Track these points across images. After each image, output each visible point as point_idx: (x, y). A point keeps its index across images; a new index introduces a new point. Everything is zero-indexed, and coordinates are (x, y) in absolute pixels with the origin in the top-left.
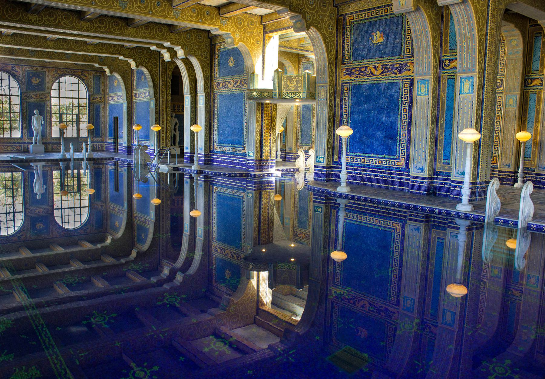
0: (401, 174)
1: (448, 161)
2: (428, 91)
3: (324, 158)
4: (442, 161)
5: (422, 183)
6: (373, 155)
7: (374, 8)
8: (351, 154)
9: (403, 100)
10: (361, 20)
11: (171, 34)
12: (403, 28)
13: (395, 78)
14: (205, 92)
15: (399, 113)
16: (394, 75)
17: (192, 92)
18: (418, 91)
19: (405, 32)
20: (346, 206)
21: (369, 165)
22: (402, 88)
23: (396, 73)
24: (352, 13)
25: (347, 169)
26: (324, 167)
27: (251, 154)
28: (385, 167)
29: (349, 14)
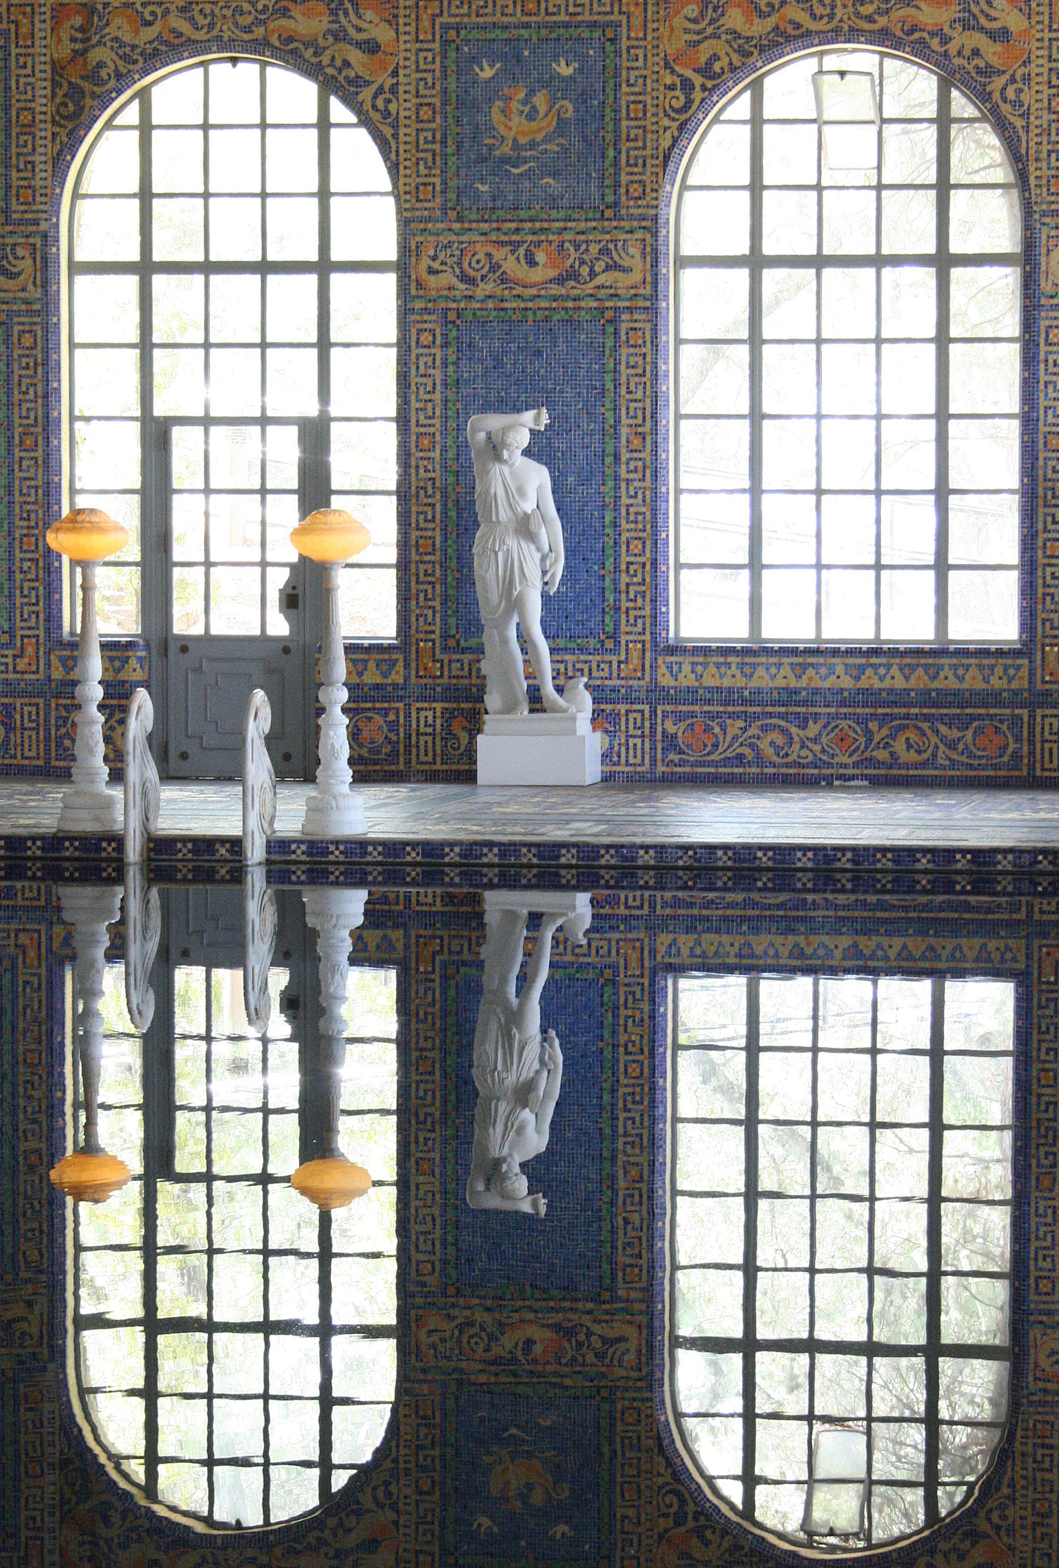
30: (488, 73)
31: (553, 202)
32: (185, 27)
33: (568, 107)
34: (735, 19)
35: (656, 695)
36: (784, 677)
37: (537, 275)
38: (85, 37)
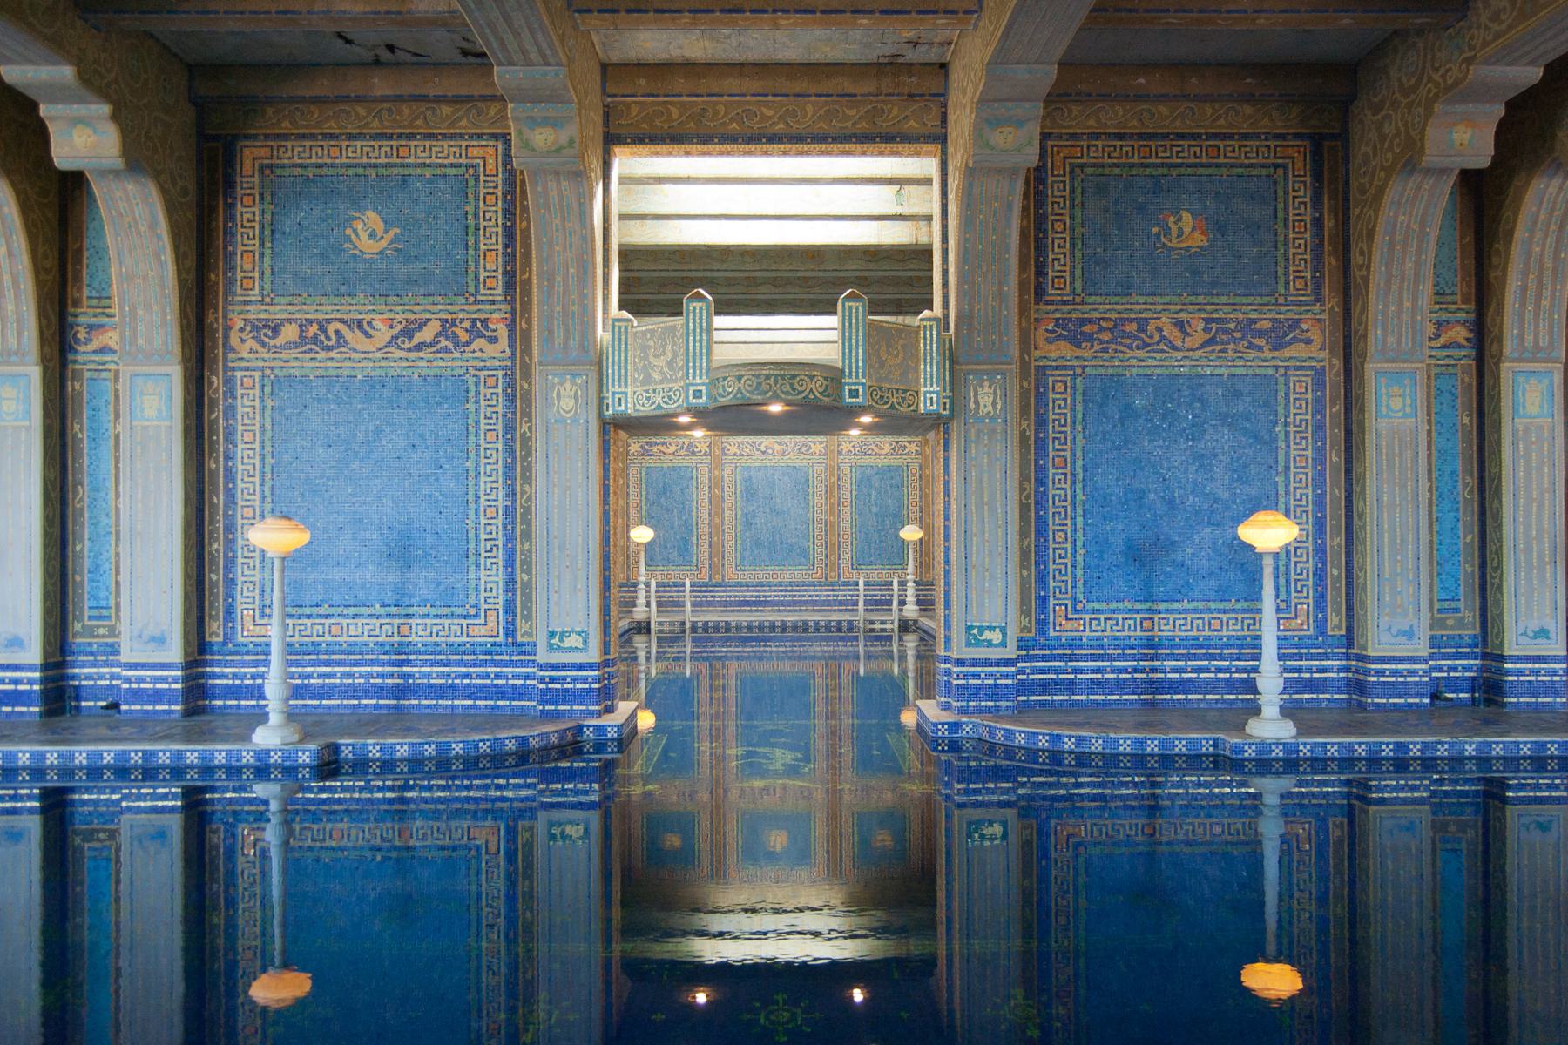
0: (1300, 657)
1: (1454, 605)
3: (1003, 630)
4: (1437, 606)
5: (1413, 673)
6: (1185, 604)
7: (1165, 136)
8: (1091, 606)
9: (1292, 429)
10: (1116, 166)
11: (79, 23)
12: (1281, 215)
14: (185, 360)
17: (47, 349)
19: (1286, 226)
22: (1287, 395)
23: (1260, 349)
24: (1073, 136)
25: (1281, 657)
26: (1007, 662)
27: (574, 641)
29: (1060, 137)
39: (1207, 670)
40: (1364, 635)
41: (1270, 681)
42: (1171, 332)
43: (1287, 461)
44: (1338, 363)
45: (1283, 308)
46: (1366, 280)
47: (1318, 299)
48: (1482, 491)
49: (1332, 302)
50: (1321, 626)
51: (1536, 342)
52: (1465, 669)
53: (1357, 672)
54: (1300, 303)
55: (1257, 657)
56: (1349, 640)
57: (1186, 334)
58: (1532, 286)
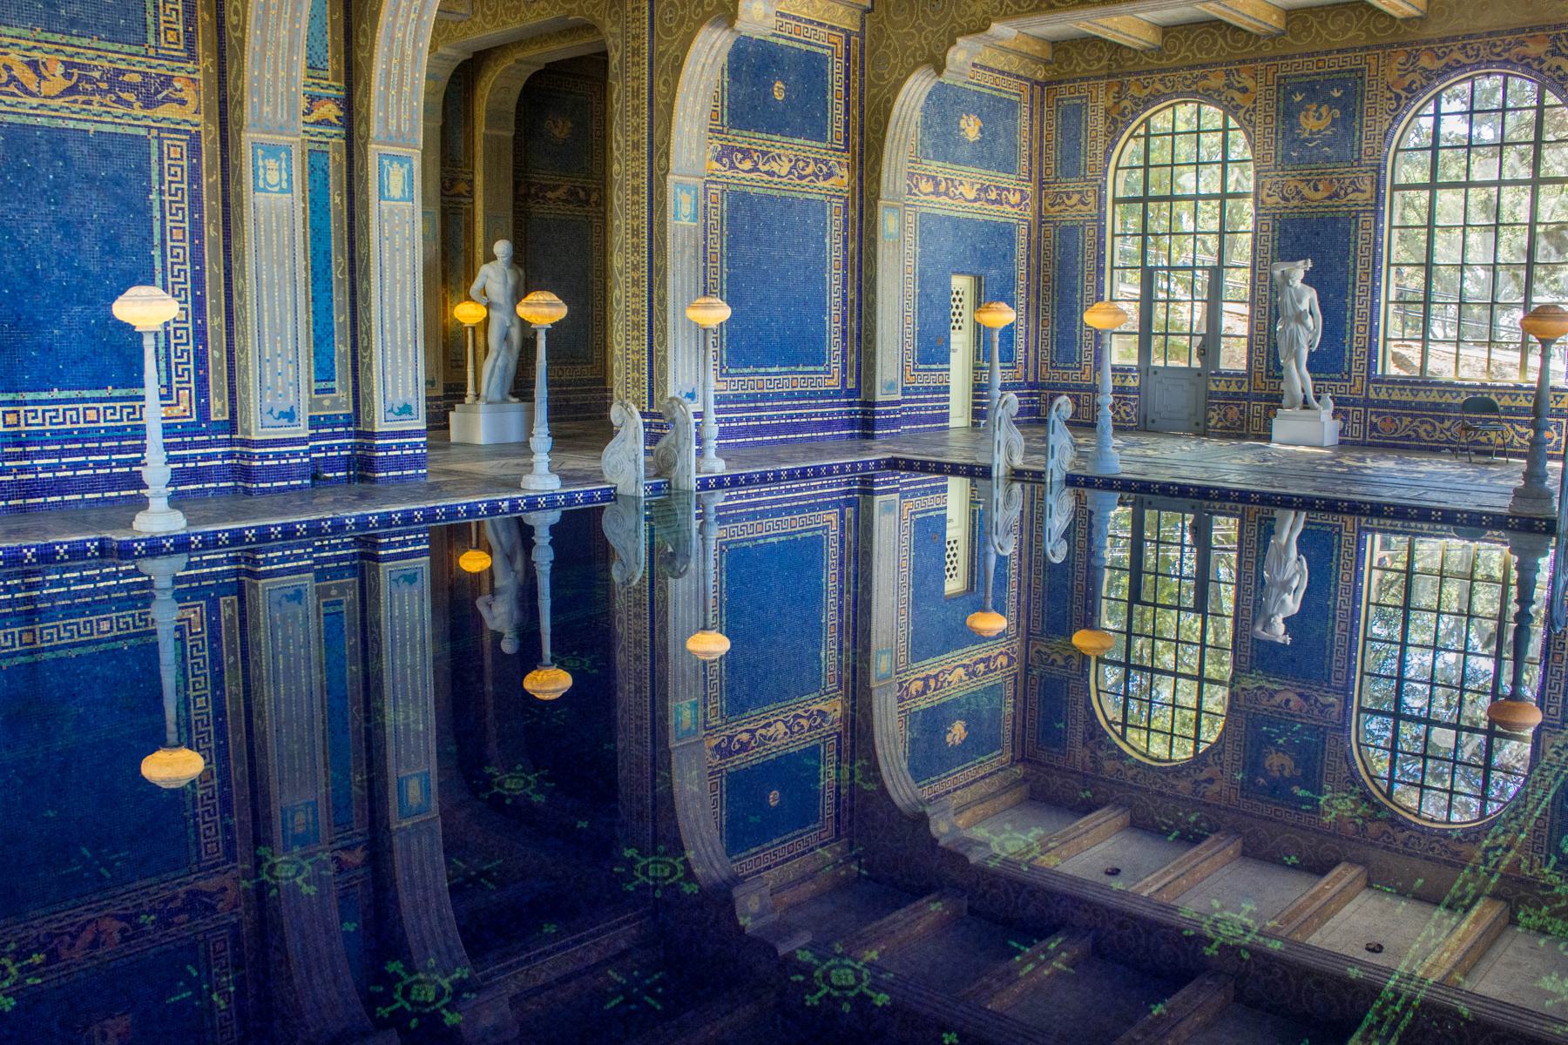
0: (184, 446)
1: (330, 385)
2: (290, 181)
4: (314, 386)
5: (295, 455)
6: (56, 394)
9: (167, 198)
13: (125, 120)
15: (157, 240)
16: (120, 110)
18: (256, 177)
20: (177, 580)
21: (43, 433)
22: (161, 159)
23: (130, 105)
25: (167, 447)
28: (117, 429)
30: (1299, 98)
31: (1328, 159)
32: (1161, 87)
33: (1337, 113)
34: (1425, 61)
35: (1368, 403)
36: (1434, 397)
37: (1319, 196)
38: (1119, 97)
39: (84, 466)
40: (247, 419)
41: (156, 470)
42: (26, 76)
43: (163, 234)
44: (214, 130)
45: (155, 62)
46: (241, 42)
47: (192, 57)
48: (352, 271)
49: (206, 62)
50: (204, 411)
51: (399, 126)
52: (342, 447)
53: (242, 457)
54: (172, 59)
55: (141, 449)
56: (232, 425)
57: (42, 77)
58: (395, 71)
